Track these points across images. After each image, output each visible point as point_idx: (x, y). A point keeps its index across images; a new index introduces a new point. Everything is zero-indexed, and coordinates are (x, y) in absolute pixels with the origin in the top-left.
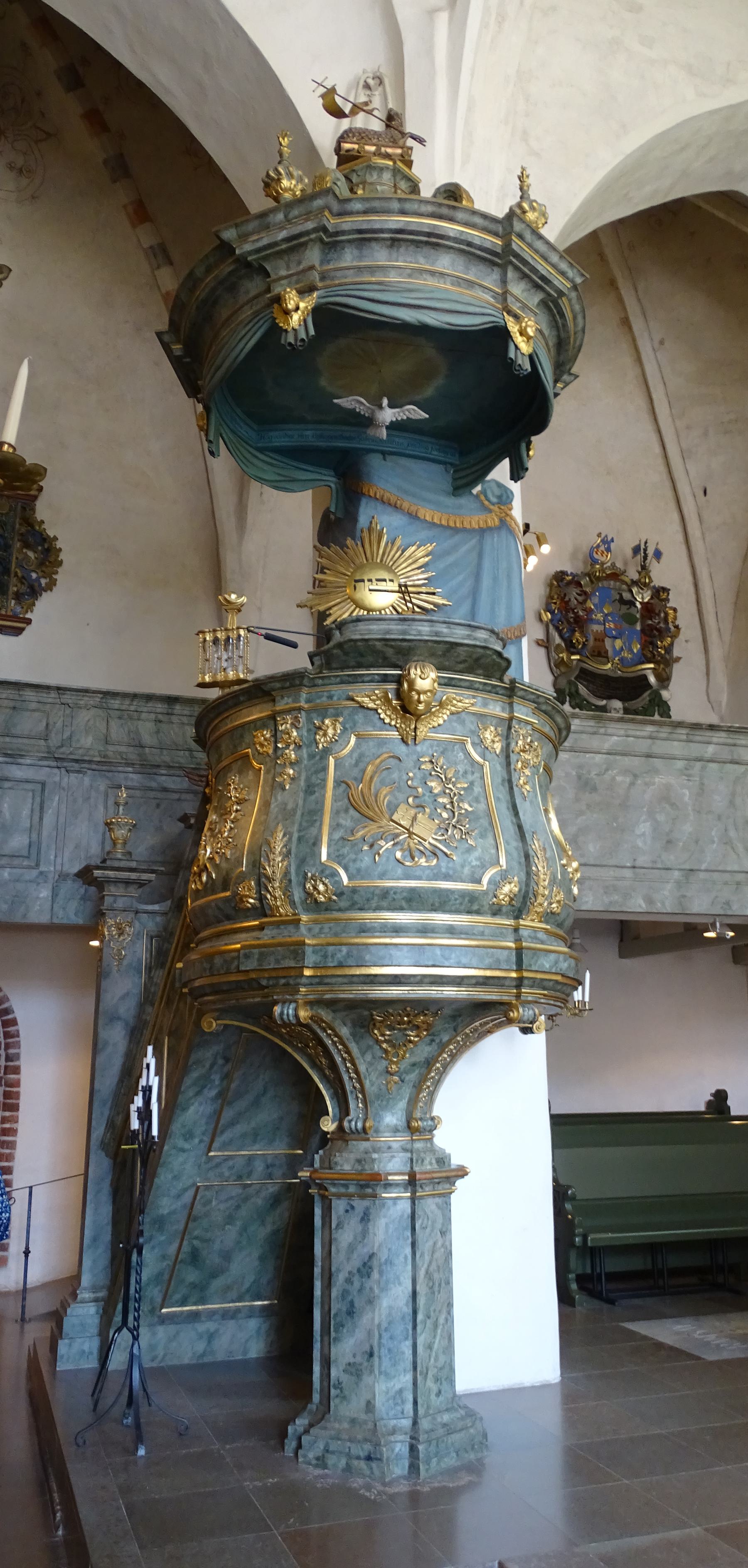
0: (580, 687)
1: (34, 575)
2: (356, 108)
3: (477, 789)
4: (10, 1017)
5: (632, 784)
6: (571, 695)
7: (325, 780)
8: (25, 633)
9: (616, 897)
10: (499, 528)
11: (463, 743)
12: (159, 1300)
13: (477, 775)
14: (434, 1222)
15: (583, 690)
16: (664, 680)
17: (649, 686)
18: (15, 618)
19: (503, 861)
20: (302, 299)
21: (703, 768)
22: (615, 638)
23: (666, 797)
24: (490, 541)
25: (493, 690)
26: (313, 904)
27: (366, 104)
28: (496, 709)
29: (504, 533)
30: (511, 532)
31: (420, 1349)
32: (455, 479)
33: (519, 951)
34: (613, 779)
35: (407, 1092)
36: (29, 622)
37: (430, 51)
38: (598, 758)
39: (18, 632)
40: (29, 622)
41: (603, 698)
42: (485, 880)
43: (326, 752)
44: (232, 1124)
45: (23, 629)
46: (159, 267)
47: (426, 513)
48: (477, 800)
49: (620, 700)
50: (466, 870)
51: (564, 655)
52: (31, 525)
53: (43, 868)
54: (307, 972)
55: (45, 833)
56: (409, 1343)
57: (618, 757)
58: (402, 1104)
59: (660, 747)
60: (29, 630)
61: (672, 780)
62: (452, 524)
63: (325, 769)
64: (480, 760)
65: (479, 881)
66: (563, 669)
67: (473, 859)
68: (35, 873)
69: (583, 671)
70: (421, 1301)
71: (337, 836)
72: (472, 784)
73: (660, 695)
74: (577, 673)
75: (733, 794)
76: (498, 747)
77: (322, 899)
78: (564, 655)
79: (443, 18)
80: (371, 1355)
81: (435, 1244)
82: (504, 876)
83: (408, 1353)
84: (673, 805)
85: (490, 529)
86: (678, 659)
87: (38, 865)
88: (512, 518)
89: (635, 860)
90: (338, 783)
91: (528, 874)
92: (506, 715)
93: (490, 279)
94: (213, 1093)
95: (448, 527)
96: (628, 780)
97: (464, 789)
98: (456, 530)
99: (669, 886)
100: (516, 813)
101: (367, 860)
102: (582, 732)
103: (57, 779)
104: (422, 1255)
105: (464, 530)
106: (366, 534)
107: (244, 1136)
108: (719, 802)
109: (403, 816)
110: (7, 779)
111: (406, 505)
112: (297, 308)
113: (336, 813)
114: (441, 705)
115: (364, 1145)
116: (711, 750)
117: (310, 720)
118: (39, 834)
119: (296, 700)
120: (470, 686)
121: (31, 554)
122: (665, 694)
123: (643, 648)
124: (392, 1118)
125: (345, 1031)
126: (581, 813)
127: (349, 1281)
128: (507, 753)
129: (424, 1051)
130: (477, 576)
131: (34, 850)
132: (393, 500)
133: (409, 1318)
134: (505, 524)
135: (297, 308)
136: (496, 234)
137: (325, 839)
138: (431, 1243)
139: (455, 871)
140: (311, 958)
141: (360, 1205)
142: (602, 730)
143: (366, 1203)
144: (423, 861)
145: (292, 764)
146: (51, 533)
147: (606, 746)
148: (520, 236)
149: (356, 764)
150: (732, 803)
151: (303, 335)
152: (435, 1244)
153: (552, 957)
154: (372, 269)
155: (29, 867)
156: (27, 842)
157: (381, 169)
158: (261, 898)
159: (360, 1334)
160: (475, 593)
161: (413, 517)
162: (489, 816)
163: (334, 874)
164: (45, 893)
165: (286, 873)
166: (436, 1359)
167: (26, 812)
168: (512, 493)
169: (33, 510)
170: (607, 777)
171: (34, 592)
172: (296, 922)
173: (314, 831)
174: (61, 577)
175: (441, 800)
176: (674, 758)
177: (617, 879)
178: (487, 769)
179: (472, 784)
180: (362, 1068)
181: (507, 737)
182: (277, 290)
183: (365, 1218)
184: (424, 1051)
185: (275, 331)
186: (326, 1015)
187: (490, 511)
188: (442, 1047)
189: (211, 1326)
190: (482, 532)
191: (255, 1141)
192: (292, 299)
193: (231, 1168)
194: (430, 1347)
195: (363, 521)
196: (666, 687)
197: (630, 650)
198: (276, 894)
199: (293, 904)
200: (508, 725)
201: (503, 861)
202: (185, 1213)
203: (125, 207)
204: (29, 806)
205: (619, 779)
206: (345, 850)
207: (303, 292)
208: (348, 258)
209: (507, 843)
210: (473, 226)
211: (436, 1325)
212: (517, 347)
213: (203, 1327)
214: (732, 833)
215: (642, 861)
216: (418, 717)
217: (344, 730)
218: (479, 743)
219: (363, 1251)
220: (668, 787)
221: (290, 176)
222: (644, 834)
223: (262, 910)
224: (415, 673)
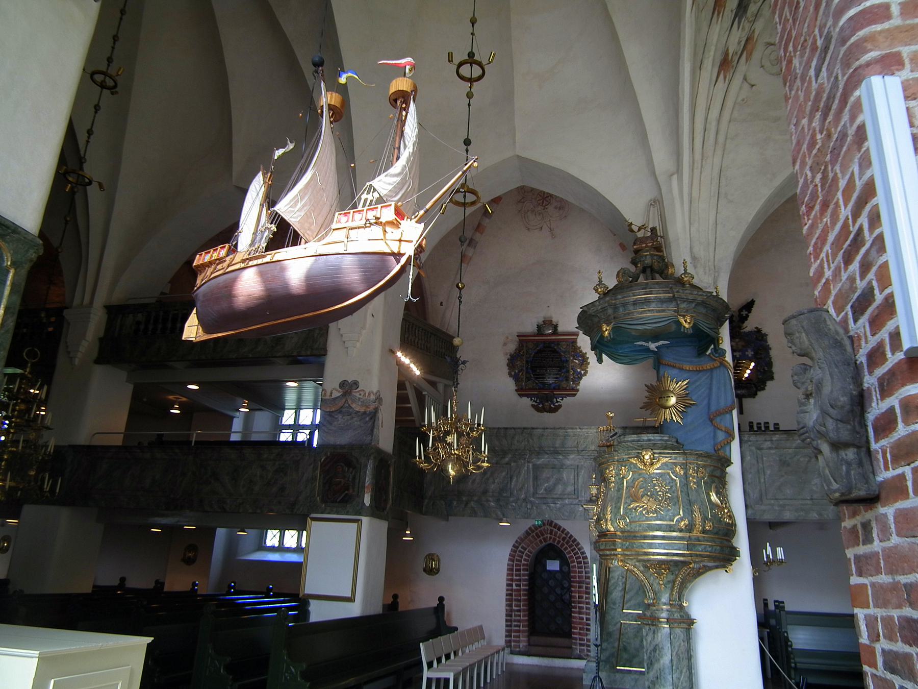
1: (579, 370)
2: (639, 229)
3: (673, 488)
5: (809, 461)
7: (623, 487)
10: (719, 367)
11: (669, 474)
12: (615, 663)
13: (674, 483)
14: (679, 637)
18: (573, 389)
19: (681, 513)
20: (608, 326)
27: (643, 226)
28: (680, 459)
31: (674, 679)
32: (698, 351)
34: (798, 460)
37: (670, 191)
38: (790, 451)
43: (623, 478)
44: (629, 600)
45: (576, 394)
47: (687, 367)
48: (674, 492)
53: (580, 499)
55: (580, 485)
56: (671, 676)
57: (801, 450)
62: (698, 369)
63: (623, 483)
64: (675, 478)
65: (673, 521)
70: (675, 663)
71: (625, 506)
72: (672, 487)
76: (682, 473)
77: (622, 526)
79: (675, 176)
80: (657, 678)
81: (680, 644)
82: (682, 519)
83: (671, 679)
85: (715, 368)
87: (578, 498)
88: (726, 361)
89: (812, 496)
93: (672, 307)
94: (620, 589)
95: (697, 370)
97: (668, 489)
98: (700, 371)
102: (781, 440)
103: (582, 463)
104: (674, 647)
105: (704, 370)
106: (663, 379)
107: (635, 605)
111: (678, 365)
112: (607, 330)
113: (626, 498)
115: (654, 608)
118: (578, 486)
126: (782, 476)
127: (650, 653)
129: (671, 577)
130: (710, 389)
133: (670, 668)
134: (723, 364)
135: (607, 330)
136: (669, 293)
137: (622, 507)
138: (678, 644)
139: (663, 518)
141: (652, 628)
142: (791, 439)
143: (654, 627)
144: (652, 515)
147: (794, 445)
148: (678, 292)
149: (632, 482)
152: (680, 644)
153: (703, 546)
155: (575, 498)
156: (573, 489)
159: (654, 671)
160: (709, 396)
161: (681, 369)
162: (678, 498)
166: (682, 683)
167: (572, 477)
168: (725, 350)
173: (619, 504)
175: (660, 493)
177: (802, 504)
178: (678, 481)
179: (672, 487)
183: (654, 633)
184: (671, 577)
185: (602, 337)
187: (715, 360)
189: (637, 676)
190: (712, 369)
191: (639, 608)
192: (605, 327)
193: (632, 617)
194: (679, 679)
195: (661, 372)
200: (684, 466)
202: (619, 631)
204: (573, 475)
206: (628, 511)
209: (683, 507)
210: (660, 294)
211: (681, 672)
212: (684, 327)
213: (633, 676)
218: (674, 473)
219: (654, 643)
222: (816, 484)
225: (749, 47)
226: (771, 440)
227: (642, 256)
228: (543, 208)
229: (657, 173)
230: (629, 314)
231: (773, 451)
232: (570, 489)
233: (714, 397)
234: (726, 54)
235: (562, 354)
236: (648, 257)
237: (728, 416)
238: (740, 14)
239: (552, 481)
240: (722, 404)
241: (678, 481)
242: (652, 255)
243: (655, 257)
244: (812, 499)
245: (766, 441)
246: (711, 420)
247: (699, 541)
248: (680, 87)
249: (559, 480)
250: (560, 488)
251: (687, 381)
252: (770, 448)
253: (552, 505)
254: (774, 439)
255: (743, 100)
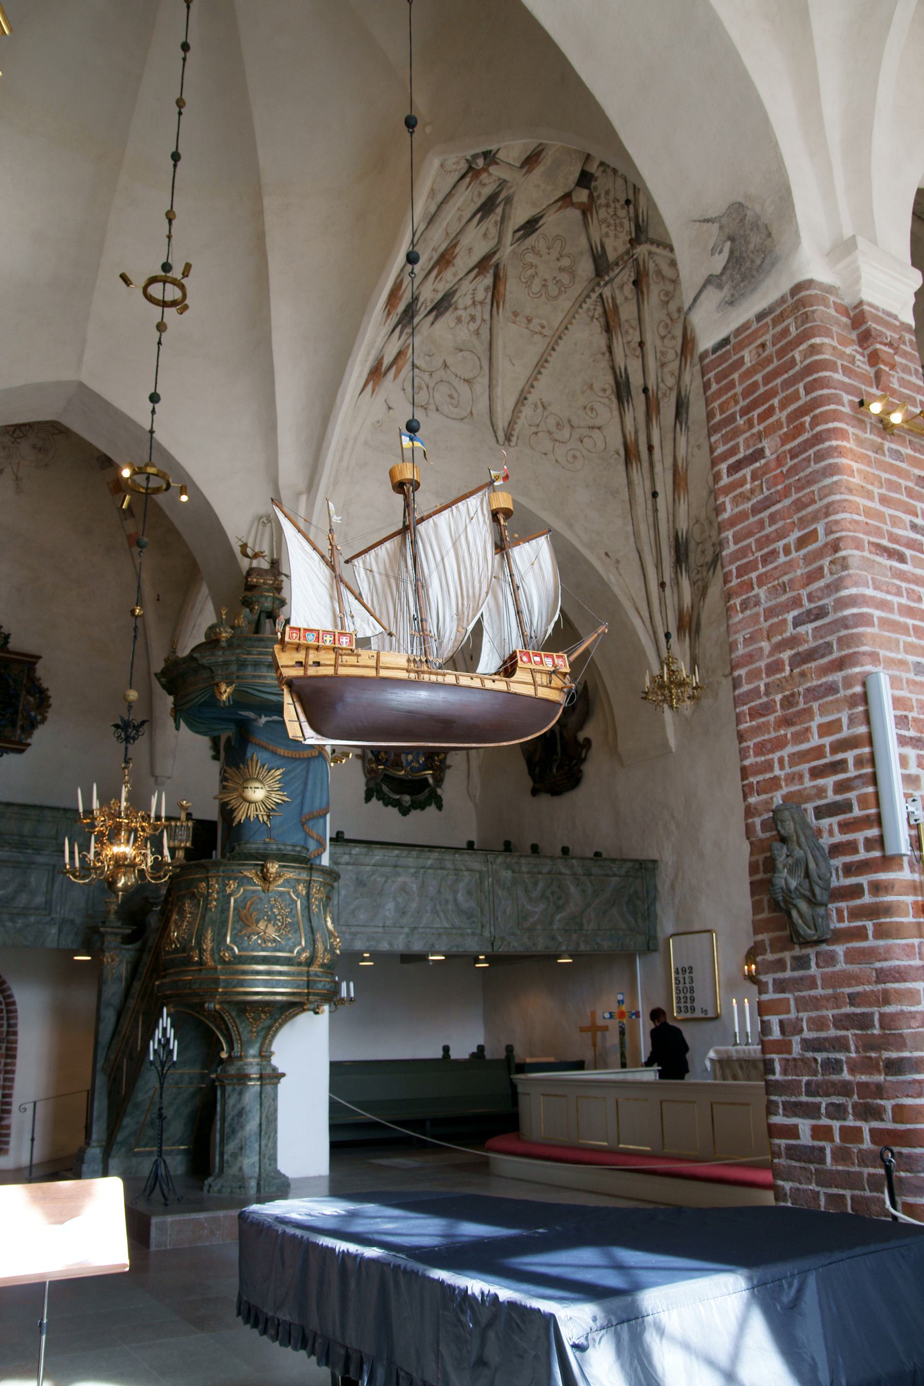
0: (384, 786)
1: (33, 714)
3: (294, 912)
4: (11, 1000)
5: (385, 882)
6: (377, 792)
7: (229, 907)
8: (26, 753)
9: (373, 943)
10: (317, 757)
11: (289, 893)
15: (385, 788)
16: (439, 781)
17: (428, 785)
18: (20, 743)
19: (303, 943)
20: (228, 687)
21: (425, 873)
22: (408, 754)
23: (403, 889)
24: (314, 764)
25: (303, 868)
26: (222, 961)
28: (304, 876)
29: (320, 759)
30: (325, 759)
33: (308, 981)
35: (260, 1040)
36: (29, 745)
38: (368, 868)
39: (21, 751)
40: (29, 745)
41: (398, 793)
42: (295, 952)
43: (230, 895)
46: (126, 519)
49: (409, 794)
50: (288, 948)
51: (374, 766)
52: (34, 682)
53: (53, 915)
54: (220, 990)
58: (257, 1045)
59: (402, 861)
60: (29, 751)
61: (407, 879)
63: (230, 902)
64: (295, 898)
65: (292, 952)
66: (373, 775)
67: (291, 943)
68: (48, 918)
69: (386, 776)
73: (436, 791)
74: (382, 777)
75: (440, 886)
76: (304, 892)
78: (374, 766)
79: (304, 498)
82: (303, 950)
84: (407, 893)
85: (313, 757)
86: (449, 767)
87: (50, 914)
88: (326, 751)
90: (235, 909)
91: (314, 948)
92: (308, 878)
95: (292, 758)
96: (383, 880)
99: (402, 937)
100: (310, 922)
101: (246, 944)
105: (300, 759)
106: (250, 763)
108: (432, 891)
109: (262, 925)
110: (33, 863)
111: (271, 747)
113: (234, 923)
114: (280, 876)
115: (240, 1063)
116: (430, 862)
117: (223, 881)
119: (218, 872)
120: (293, 867)
121: (31, 699)
122: (439, 791)
123: (426, 760)
124: (253, 1051)
125: (234, 1014)
126: (357, 898)
128: (308, 894)
129: (268, 1022)
131: (48, 906)
132: (264, 744)
140: (222, 984)
145: (215, 900)
146: (45, 685)
147: (373, 862)
150: (439, 891)
151: (227, 704)
154: (260, 677)
157: (267, 597)
158: (201, 958)
161: (274, 753)
162: (298, 923)
163: (233, 949)
164: (54, 931)
165: (212, 949)
167: (44, 883)
169: (35, 672)
170: (372, 878)
171: (32, 725)
172: (216, 969)
174: (50, 715)
176: (409, 867)
178: (299, 903)
179: (292, 909)
180: (241, 1030)
181: (308, 888)
182: (217, 680)
184: (268, 1022)
186: (226, 1007)
188: (276, 1021)
192: (223, 687)
195: (249, 754)
196: (440, 786)
197: (418, 762)
198: (207, 957)
199: (215, 961)
200: (309, 884)
201: (303, 943)
203: (108, 483)
205: (378, 879)
207: (228, 685)
208: (249, 671)
214: (438, 908)
215: (388, 923)
216: (270, 882)
217: (239, 886)
220: (405, 883)
221: (226, 632)
223: (201, 963)
224: (269, 865)
225: (400, 362)
226: (350, 854)
227: (262, 596)
228: (13, 440)
229: (281, 482)
230: (260, 677)
231: (350, 867)
232: (40, 900)
233: (308, 794)
234: (380, 362)
235: (11, 683)
236: (269, 599)
237: (321, 821)
238: (404, 322)
239: (12, 888)
240: (317, 805)
241: (299, 903)
242: (274, 598)
243: (277, 602)
244: (384, 927)
245: (344, 854)
246: (303, 824)
247: (319, 977)
248: (341, 390)
249: (23, 886)
250: (23, 899)
251: (281, 771)
252: (348, 864)
253: (9, 924)
254: (354, 852)
255: (378, 422)
